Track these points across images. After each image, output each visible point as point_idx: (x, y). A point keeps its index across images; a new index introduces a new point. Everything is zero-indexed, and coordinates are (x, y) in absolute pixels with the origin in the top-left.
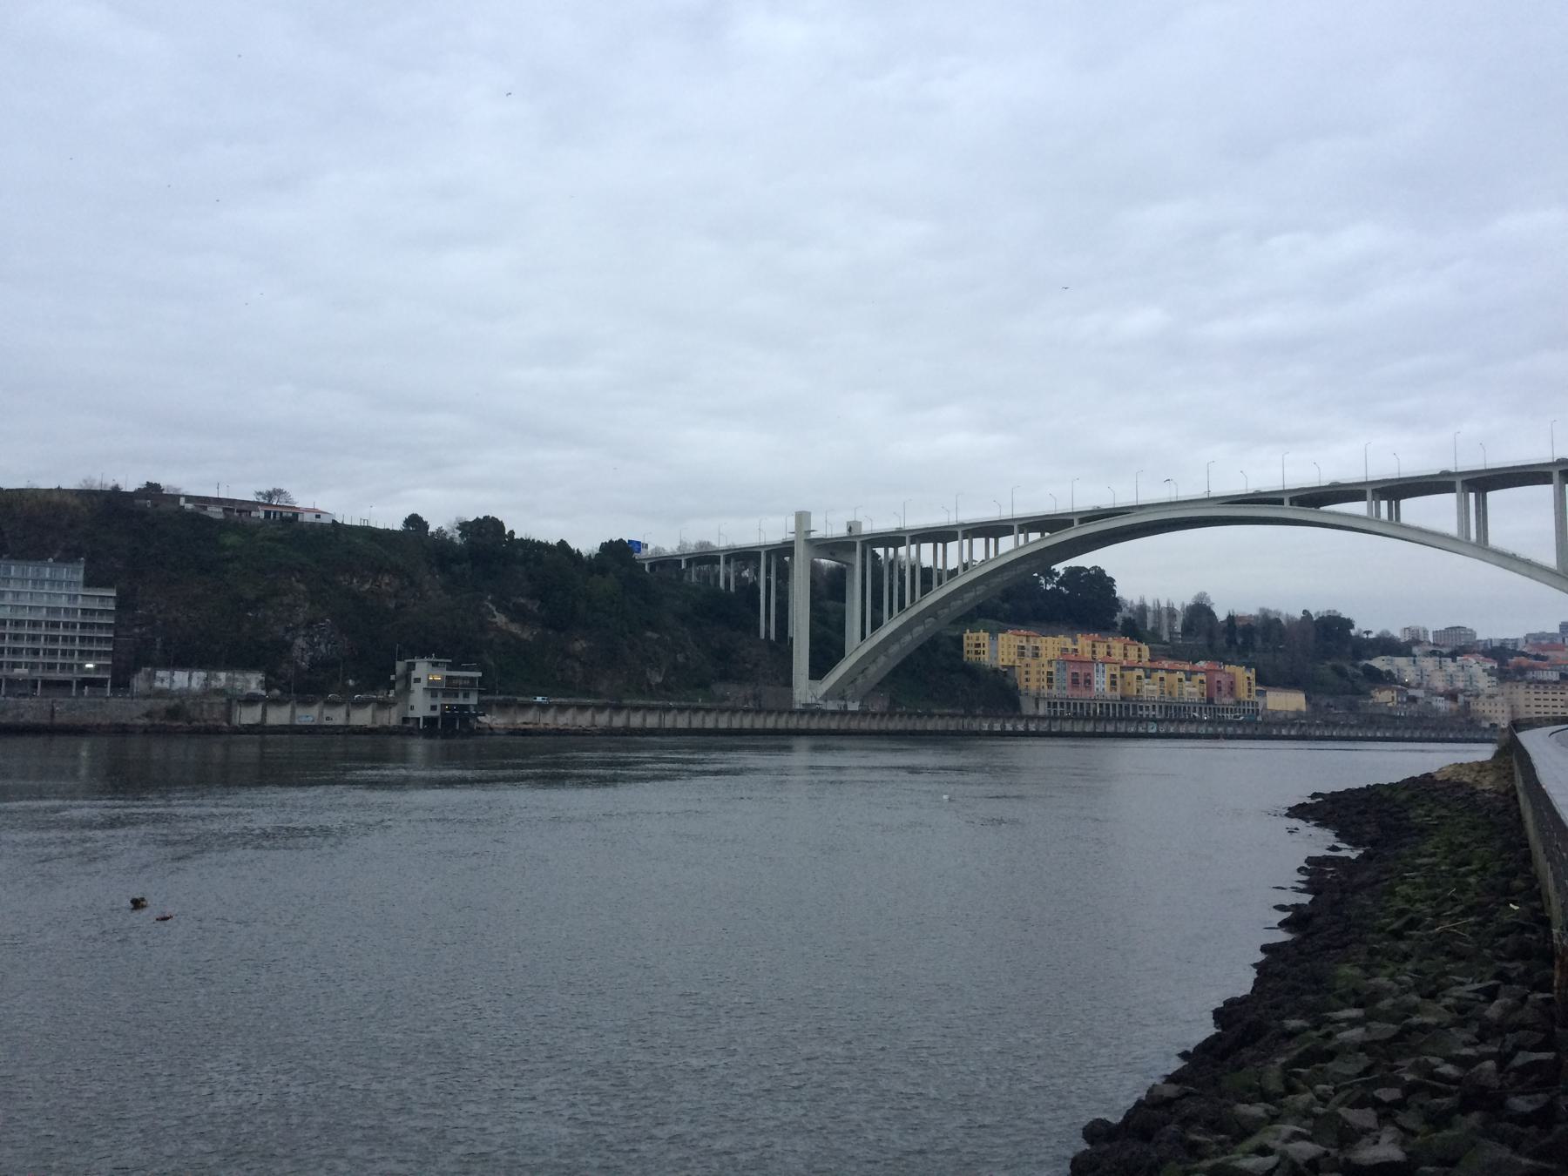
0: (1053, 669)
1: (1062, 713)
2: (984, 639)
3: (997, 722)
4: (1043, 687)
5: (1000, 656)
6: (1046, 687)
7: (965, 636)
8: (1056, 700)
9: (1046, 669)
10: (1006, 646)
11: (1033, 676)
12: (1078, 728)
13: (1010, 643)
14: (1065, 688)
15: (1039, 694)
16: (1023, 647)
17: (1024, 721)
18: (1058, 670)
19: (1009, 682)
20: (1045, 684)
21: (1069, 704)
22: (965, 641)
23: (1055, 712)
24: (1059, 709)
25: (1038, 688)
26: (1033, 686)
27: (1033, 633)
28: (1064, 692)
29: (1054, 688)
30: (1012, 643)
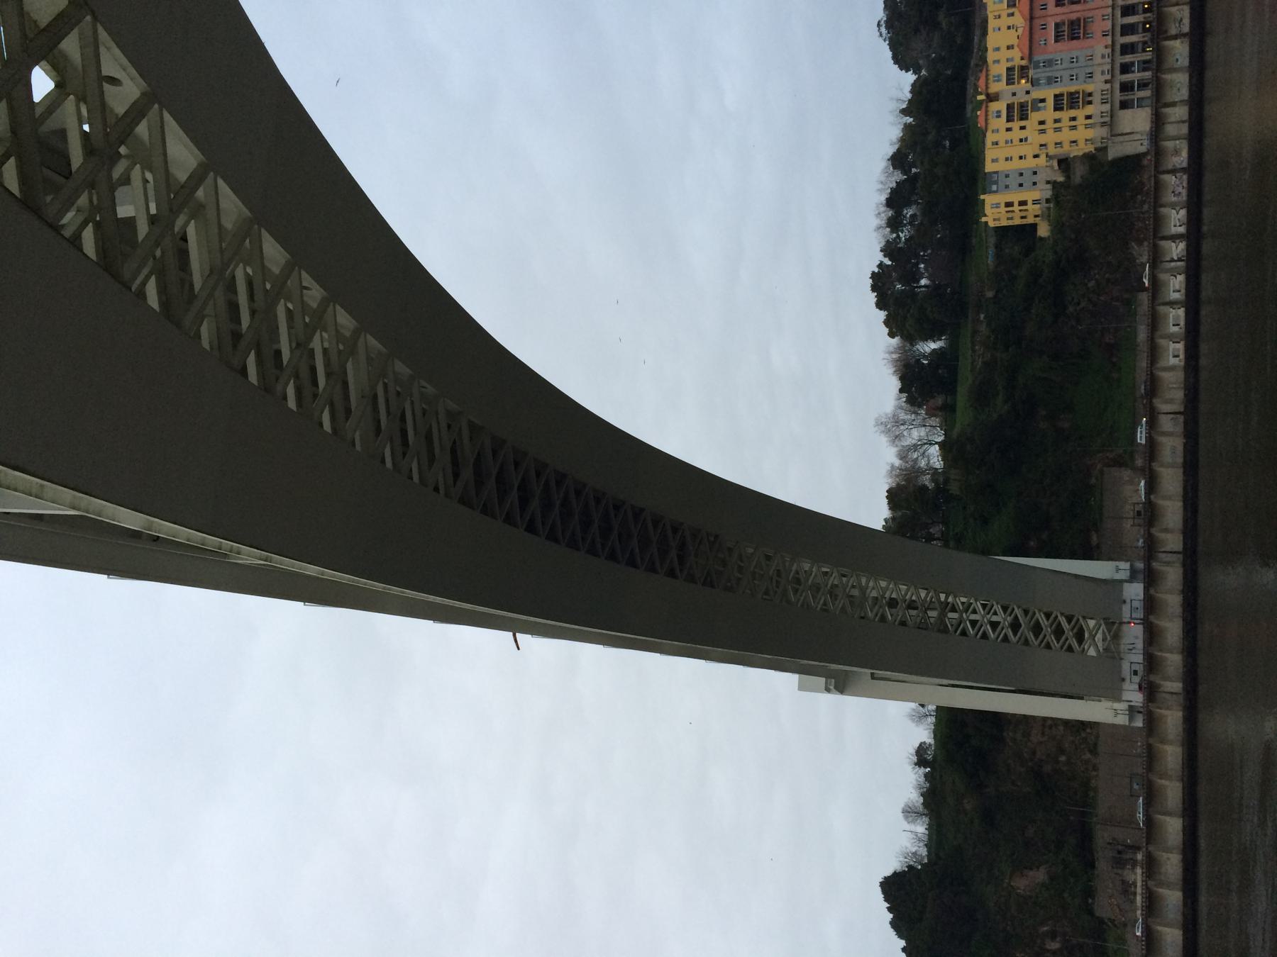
0: (1049, 93)
1: (1145, 65)
2: (997, 206)
3: (1166, 316)
4: (1088, 117)
5: (1030, 163)
6: (1089, 110)
7: (991, 224)
8: (1117, 86)
9: (1048, 113)
11: (1066, 136)
12: (1179, 84)
14: (1091, 58)
17: (1165, 244)
18: (1051, 81)
19: (1079, 172)
20: (1080, 113)
21: (1127, 49)
22: (1004, 223)
23: (1143, 85)
24: (1135, 76)
25: (1087, 126)
26: (1082, 134)
27: (982, 83)
28: (1098, 60)
29: (1089, 88)
30: (1002, 136)
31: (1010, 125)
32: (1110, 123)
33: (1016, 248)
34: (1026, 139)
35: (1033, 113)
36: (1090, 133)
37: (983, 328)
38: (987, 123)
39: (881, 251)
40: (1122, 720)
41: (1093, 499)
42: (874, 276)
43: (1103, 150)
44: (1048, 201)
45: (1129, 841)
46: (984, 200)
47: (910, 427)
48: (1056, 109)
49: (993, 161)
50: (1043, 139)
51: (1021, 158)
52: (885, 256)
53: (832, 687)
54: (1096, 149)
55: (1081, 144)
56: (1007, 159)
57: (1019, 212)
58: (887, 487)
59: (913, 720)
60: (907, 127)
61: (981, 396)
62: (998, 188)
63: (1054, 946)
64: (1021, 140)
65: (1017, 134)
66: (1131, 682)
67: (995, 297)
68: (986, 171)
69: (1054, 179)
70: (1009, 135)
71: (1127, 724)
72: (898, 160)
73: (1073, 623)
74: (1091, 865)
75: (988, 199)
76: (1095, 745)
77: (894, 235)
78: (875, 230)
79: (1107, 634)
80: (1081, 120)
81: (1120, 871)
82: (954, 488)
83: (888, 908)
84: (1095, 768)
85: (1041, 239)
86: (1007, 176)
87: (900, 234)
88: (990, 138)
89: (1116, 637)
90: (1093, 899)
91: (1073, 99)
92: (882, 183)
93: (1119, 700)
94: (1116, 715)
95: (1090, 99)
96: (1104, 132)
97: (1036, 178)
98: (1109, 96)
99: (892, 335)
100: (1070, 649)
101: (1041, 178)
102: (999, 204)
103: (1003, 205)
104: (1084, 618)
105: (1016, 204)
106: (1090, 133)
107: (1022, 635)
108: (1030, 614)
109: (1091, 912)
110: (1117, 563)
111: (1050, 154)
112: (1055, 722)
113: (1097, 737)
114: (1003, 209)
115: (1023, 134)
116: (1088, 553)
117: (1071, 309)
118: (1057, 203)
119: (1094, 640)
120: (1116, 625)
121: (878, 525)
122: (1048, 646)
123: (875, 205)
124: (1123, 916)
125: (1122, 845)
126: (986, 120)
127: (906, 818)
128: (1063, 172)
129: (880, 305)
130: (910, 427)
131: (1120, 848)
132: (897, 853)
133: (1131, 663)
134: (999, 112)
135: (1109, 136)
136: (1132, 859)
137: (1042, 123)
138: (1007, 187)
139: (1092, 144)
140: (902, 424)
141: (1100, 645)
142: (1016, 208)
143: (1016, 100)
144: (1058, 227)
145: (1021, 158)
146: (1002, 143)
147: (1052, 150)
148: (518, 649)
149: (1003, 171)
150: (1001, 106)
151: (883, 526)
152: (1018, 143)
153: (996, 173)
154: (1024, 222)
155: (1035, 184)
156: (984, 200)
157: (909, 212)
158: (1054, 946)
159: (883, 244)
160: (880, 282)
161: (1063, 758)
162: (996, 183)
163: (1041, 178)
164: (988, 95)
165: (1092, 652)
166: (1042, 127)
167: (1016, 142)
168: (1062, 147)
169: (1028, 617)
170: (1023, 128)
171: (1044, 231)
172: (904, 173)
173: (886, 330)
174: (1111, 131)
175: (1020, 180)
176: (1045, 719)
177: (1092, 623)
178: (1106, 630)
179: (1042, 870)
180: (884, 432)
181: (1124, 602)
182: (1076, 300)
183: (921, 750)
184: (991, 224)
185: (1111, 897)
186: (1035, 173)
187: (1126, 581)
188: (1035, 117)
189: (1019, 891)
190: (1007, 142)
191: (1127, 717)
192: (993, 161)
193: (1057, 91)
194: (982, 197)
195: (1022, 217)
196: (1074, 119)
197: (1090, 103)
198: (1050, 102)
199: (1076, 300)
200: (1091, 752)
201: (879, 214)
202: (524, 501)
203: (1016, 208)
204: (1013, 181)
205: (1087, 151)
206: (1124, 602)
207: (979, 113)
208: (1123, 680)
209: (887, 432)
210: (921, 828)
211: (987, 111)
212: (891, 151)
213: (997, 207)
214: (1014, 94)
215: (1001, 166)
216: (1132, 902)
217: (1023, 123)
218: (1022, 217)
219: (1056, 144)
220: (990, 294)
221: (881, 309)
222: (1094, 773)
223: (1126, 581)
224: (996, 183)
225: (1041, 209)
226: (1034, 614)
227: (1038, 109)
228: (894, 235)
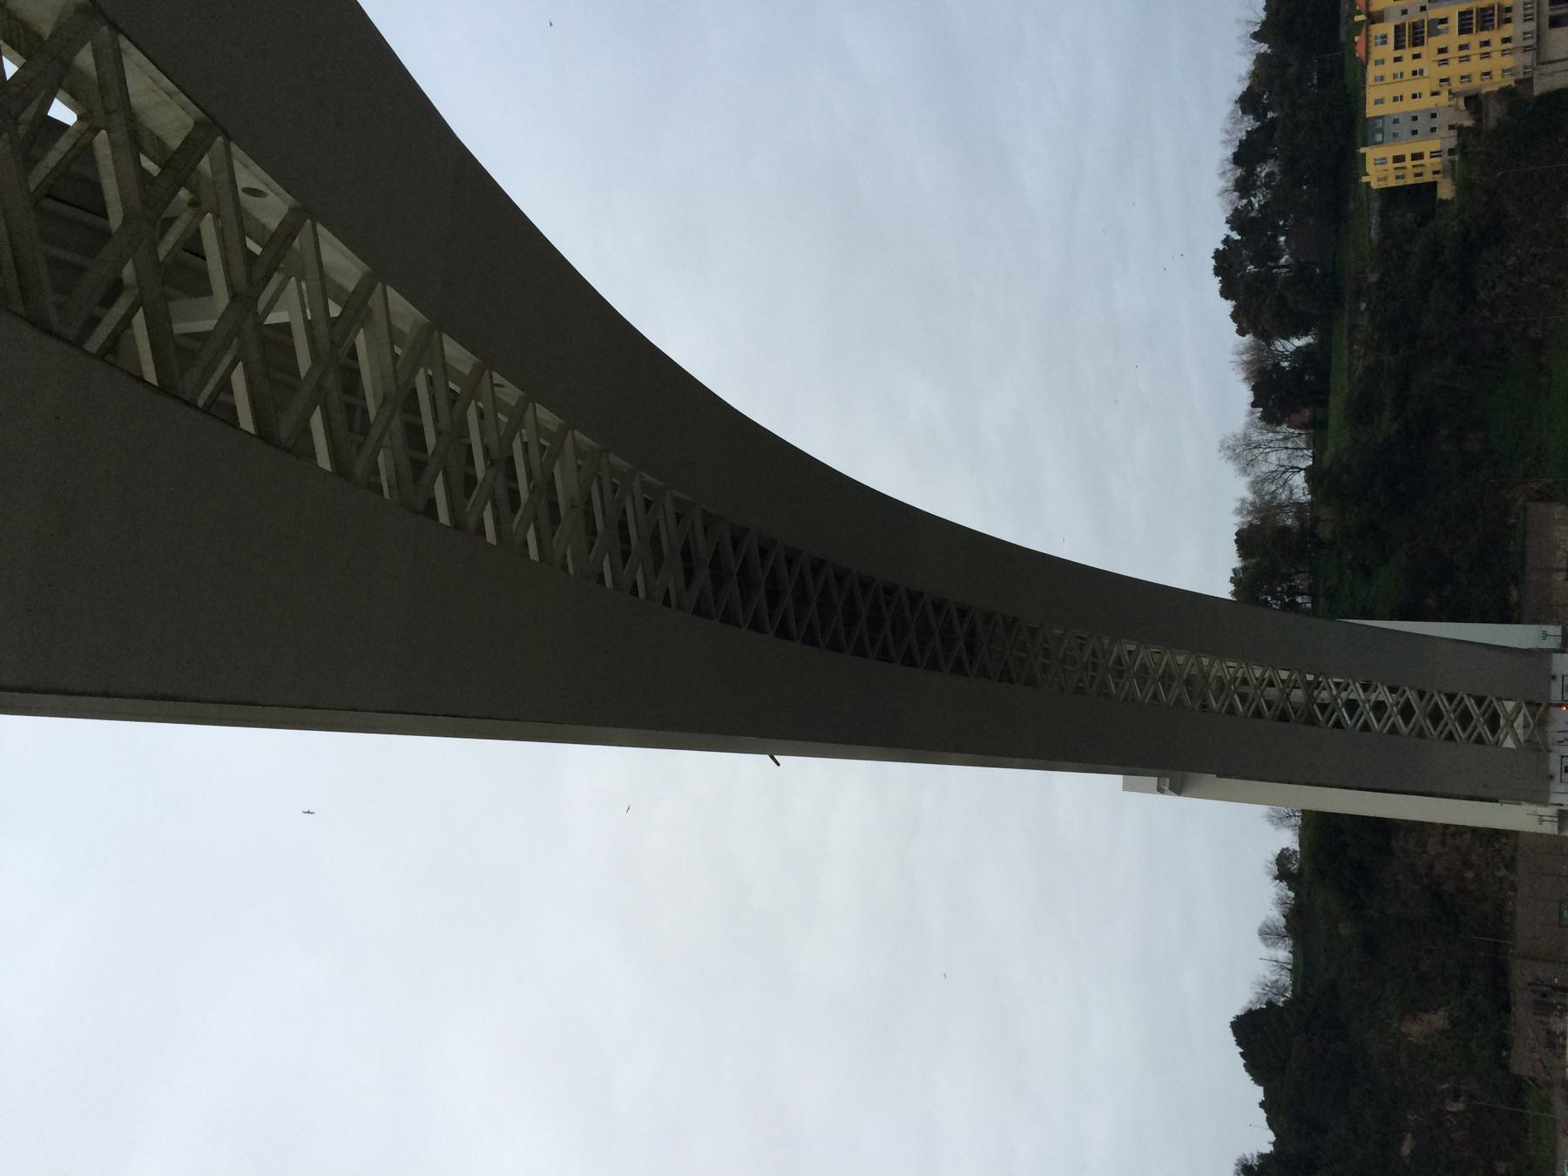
2: (1383, 161)
4: (1506, 40)
5: (1427, 102)
6: (1508, 30)
9: (1451, 37)
10: (1397, 90)
11: (1476, 66)
13: (1388, 78)
15: (1526, 49)
16: (1399, 30)
19: (1494, 113)
20: (1494, 36)
22: (1392, 183)
25: (1504, 53)
30: (1390, 69)
31: (1398, 53)
32: (1537, 47)
33: (1409, 215)
34: (1421, 72)
35: (1430, 39)
36: (1508, 62)
37: (1364, 321)
38: (1368, 53)
39: (1227, 222)
40: (1550, 828)
41: (1512, 543)
42: (1218, 255)
43: (1527, 82)
44: (1451, 152)
45: (1556, 980)
46: (1364, 154)
47: (1267, 450)
48: (1461, 32)
49: (1376, 102)
50: (1444, 72)
51: (1414, 96)
52: (1232, 229)
53: (1166, 788)
54: (1515, 82)
55: (1497, 76)
56: (1395, 99)
57: (1411, 167)
58: (1236, 529)
59: (1273, 822)
60: (1261, 59)
61: (1362, 410)
62: (1383, 137)
63: (1458, 1107)
64: (1415, 73)
65: (1408, 65)
66: (1561, 781)
67: (1381, 280)
68: (1367, 116)
69: (1460, 123)
70: (1398, 67)
71: (1556, 833)
72: (1248, 102)
73: (1484, 707)
74: (1506, 1007)
75: (1371, 154)
76: (1513, 858)
77: (1245, 201)
78: (1219, 195)
79: (1530, 719)
80: (1497, 45)
81: (1545, 1020)
82: (1325, 532)
83: (1241, 1053)
84: (1513, 887)
85: (1444, 202)
86: (1396, 121)
87: (1253, 199)
88: (1372, 72)
89: (1542, 723)
90: (1509, 1050)
91: (1485, 16)
92: (1227, 132)
93: (1545, 803)
94: (1541, 821)
95: (1508, 15)
96: (1528, 58)
97: (1436, 123)
98: (1534, 11)
99: (1241, 332)
100: (1480, 740)
101: (1441, 121)
102: (1385, 159)
103: (1390, 160)
104: (1499, 699)
105: (1408, 158)
106: (1508, 62)
107: (1415, 725)
108: (1427, 696)
109: (1505, 1067)
110: (1544, 628)
111: (1453, 91)
112: (1460, 830)
113: (1516, 848)
114: (1390, 165)
115: (1417, 65)
116: (1505, 614)
117: (1483, 294)
118: (1464, 156)
119: (1512, 726)
120: (1542, 708)
121: (1223, 589)
122: (1450, 737)
123: (1219, 163)
124: (1549, 1074)
125: (1547, 986)
126: (1367, 47)
127: (1264, 940)
128: (1471, 114)
129: (1226, 293)
130: (1267, 450)
131: (1544, 989)
132: (1253, 983)
133: (1562, 757)
134: (1384, 37)
135: (1535, 65)
136: (1559, 1004)
137: (1442, 51)
138: (1395, 135)
139: (1512, 75)
140: (1255, 448)
141: (1520, 731)
142: (1408, 163)
143: (1406, 20)
144: (1464, 187)
145: (1414, 96)
146: (1388, 78)
147: (1456, 85)
148: (778, 764)
149: (1389, 115)
150: (1387, 28)
151: (1232, 578)
152: (1410, 76)
153: (1379, 117)
154: (1419, 180)
155: (1433, 130)
156: (1364, 154)
157: (1263, 170)
158: (1458, 1107)
159: (1229, 213)
160: (1225, 263)
161: (1470, 875)
162: (1381, 131)
163: (1441, 121)
164: (1369, 15)
165: (1509, 743)
166: (1443, 56)
167: (1408, 75)
168: (1470, 81)
169: (1424, 701)
170: (1416, 56)
171: (1446, 191)
172: (1257, 119)
173: (1234, 326)
174: (1537, 58)
175: (1415, 125)
176: (1446, 826)
177: (1510, 706)
178: (1528, 715)
179: (1441, 1013)
180: (1231, 457)
181: (1554, 677)
182: (1490, 284)
183: (1283, 858)
184: (1375, 185)
185: (1532, 1051)
186: (1434, 116)
187: (1556, 651)
188: (1433, 43)
189: (1411, 1039)
190: (1395, 76)
191: (1556, 824)
192: (1376, 102)
193: (1464, 7)
194: (1362, 150)
195: (1417, 175)
196: (1486, 43)
197: (1508, 21)
198: (1454, 22)
199: (1490, 284)
200: (1507, 867)
201: (1224, 173)
202: (774, 596)
203: (1408, 163)
204: (1405, 128)
205: (1504, 84)
206: (1554, 677)
207: (1357, 39)
208: (1552, 777)
209: (1236, 457)
210: (1283, 953)
211: (1367, 36)
212: (1240, 88)
213: (1382, 164)
214: (1404, 12)
215: (1389, 109)
216: (1559, 1057)
217: (1416, 50)
218: (1417, 175)
219: (1462, 77)
220: (1373, 278)
221: (1227, 298)
222: (1512, 894)
223: (1556, 651)
224: (1381, 131)
225: (1442, 162)
226: (1432, 696)
227: (1438, 33)
228: (1245, 201)
